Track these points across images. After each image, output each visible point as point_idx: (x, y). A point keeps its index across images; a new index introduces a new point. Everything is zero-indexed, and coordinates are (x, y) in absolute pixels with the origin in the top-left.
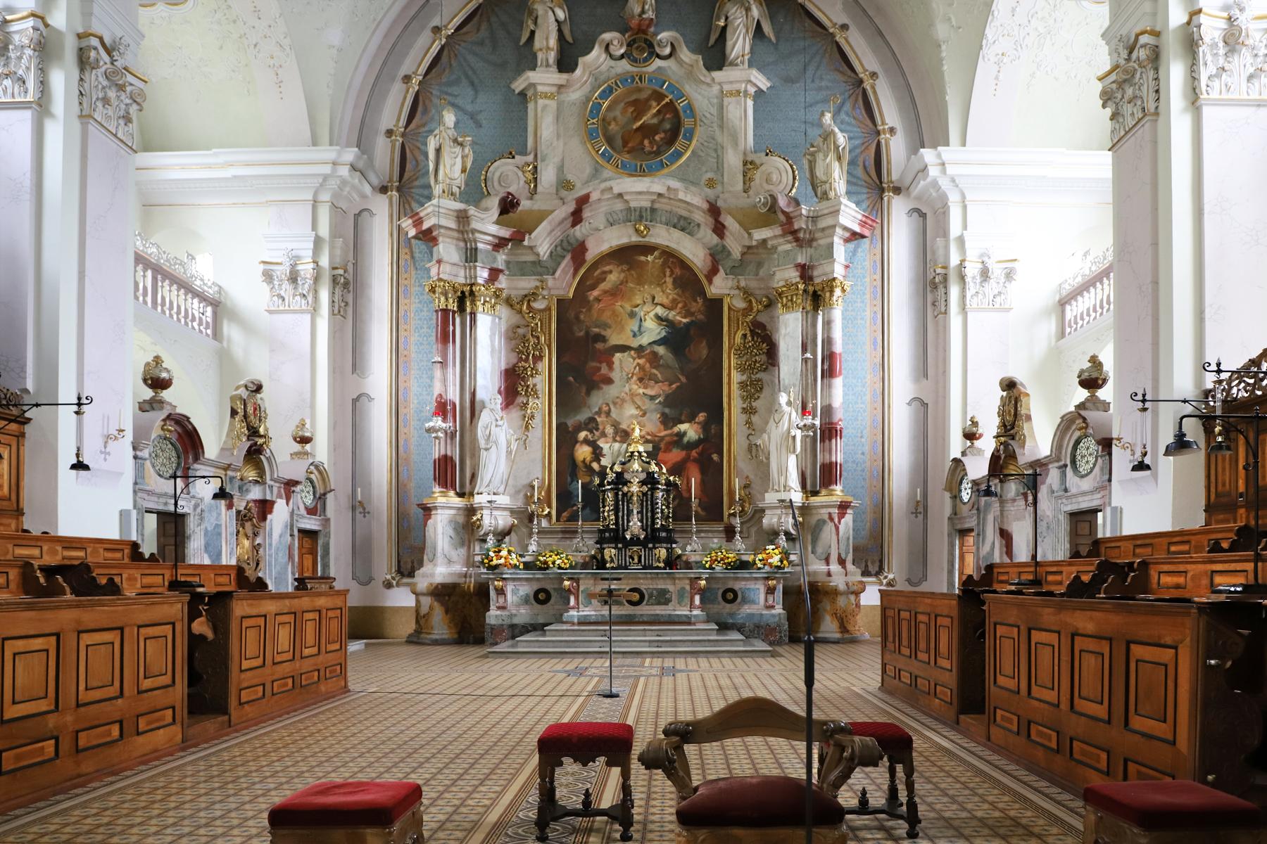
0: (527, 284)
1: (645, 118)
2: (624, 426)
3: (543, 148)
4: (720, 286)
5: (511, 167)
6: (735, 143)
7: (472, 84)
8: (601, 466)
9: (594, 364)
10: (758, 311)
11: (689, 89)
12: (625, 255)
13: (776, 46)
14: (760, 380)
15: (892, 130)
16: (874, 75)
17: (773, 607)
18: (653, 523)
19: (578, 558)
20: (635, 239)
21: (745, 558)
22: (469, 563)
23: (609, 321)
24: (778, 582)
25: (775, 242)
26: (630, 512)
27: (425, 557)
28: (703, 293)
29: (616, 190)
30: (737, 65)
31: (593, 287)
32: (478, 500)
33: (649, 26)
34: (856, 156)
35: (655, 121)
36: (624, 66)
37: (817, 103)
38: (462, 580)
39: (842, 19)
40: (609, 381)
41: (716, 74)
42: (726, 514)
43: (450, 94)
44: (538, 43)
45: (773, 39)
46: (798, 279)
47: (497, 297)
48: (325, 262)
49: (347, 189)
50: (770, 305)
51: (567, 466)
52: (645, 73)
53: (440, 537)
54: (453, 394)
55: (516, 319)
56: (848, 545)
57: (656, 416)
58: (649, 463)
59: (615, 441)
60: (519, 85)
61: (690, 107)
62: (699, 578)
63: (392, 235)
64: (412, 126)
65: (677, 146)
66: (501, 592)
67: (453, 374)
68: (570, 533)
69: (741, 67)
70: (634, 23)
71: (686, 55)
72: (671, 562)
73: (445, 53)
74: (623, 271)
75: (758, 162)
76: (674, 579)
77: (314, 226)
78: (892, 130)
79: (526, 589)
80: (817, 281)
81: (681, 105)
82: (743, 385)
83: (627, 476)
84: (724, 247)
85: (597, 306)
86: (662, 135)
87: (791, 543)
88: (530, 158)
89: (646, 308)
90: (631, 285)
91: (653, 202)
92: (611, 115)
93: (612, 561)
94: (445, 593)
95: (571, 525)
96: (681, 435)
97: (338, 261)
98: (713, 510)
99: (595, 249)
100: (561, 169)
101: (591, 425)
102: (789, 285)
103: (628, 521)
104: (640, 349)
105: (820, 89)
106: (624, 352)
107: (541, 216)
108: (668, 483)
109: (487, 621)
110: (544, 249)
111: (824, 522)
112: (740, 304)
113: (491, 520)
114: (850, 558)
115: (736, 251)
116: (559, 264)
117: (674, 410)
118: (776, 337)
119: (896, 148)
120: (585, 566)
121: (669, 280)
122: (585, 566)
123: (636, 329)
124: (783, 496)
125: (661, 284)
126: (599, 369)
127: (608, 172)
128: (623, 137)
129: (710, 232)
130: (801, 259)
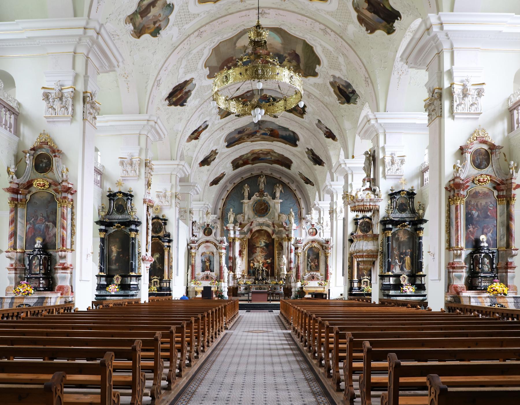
0: (243, 236)
3: (245, 212)
4: (274, 236)
11: (269, 202)
12: (258, 231)
15: (303, 208)
16: (300, 199)
20: (260, 228)
22: (234, 283)
28: (271, 237)
36: (259, 198)
39: (295, 189)
40: (256, 253)
44: (245, 194)
51: (249, 267)
54: (232, 256)
55: (241, 242)
60: (242, 201)
61: (269, 206)
65: (267, 212)
66: (240, 288)
67: (232, 252)
68: (249, 278)
70: (261, 191)
71: (269, 197)
78: (303, 208)
79: (244, 288)
82: (278, 253)
95: (250, 277)
96: (268, 262)
98: (273, 275)
99: (254, 230)
100: (248, 216)
101: (253, 260)
104: (261, 247)
107: (245, 225)
112: (277, 239)
113: (238, 276)
117: (267, 257)
119: (304, 211)
125: (264, 236)
127: (256, 217)
130: (287, 233)
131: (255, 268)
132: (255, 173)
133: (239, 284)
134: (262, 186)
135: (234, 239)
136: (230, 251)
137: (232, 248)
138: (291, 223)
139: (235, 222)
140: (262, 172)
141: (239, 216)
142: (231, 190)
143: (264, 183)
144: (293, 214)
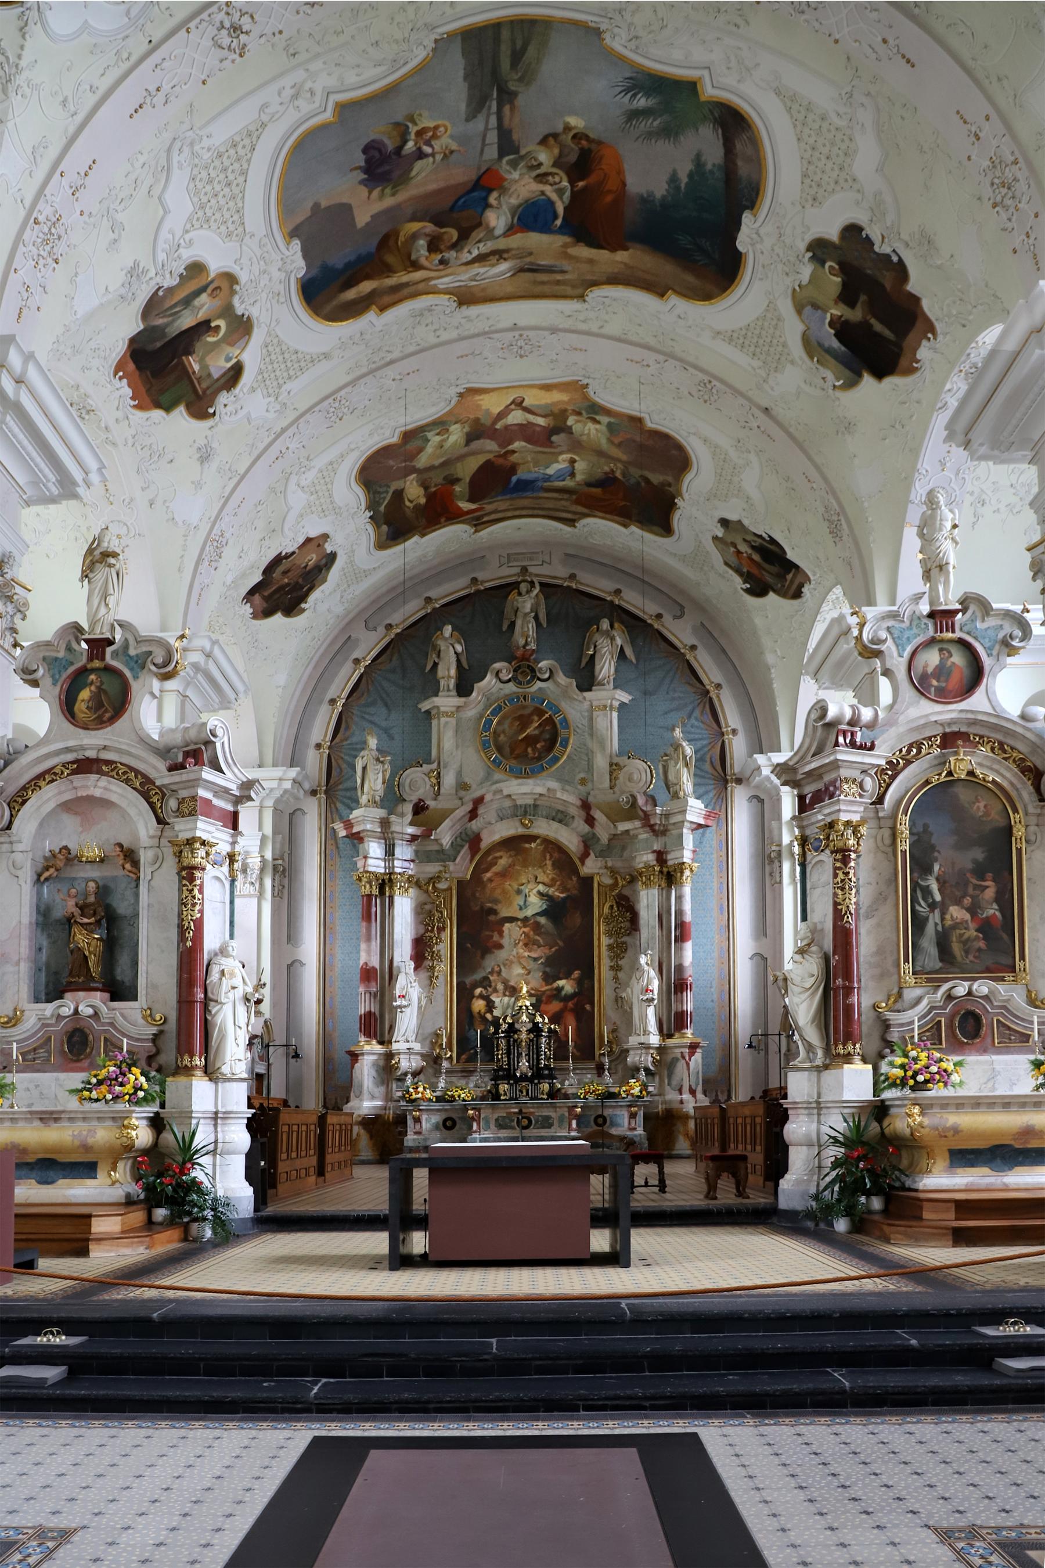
0: (433, 868)
1: (528, 731)
2: (512, 983)
3: (444, 757)
4: (591, 866)
5: (420, 774)
6: (602, 747)
7: (386, 705)
8: (494, 1017)
9: (487, 933)
10: (623, 886)
11: (564, 705)
12: (512, 844)
13: (636, 666)
14: (625, 943)
17: (635, 1129)
18: (538, 1063)
19: (479, 1092)
20: (521, 831)
21: (612, 1090)
22: (388, 1097)
23: (500, 897)
24: (640, 1109)
25: (635, 832)
26: (519, 1055)
27: (352, 1094)
28: (576, 872)
29: (505, 793)
30: (604, 685)
31: (487, 870)
32: (395, 1046)
33: (531, 655)
34: (705, 754)
35: (537, 732)
36: (511, 687)
37: (672, 711)
38: (382, 1112)
39: (691, 640)
40: (500, 947)
41: (587, 694)
42: (597, 1053)
43: (368, 714)
44: (441, 672)
45: (634, 660)
46: (655, 863)
47: (410, 882)
48: (269, 855)
49: (287, 796)
50: (633, 880)
51: (466, 1017)
52: (529, 693)
53: (366, 1077)
54: (375, 962)
55: (423, 897)
56: (698, 1078)
57: (539, 974)
58: (534, 1015)
59: (505, 995)
60: (425, 706)
61: (565, 721)
62: (576, 1107)
63: (320, 830)
64: (337, 740)
65: (555, 752)
67: (376, 945)
68: (467, 1073)
69: (607, 687)
70: (519, 653)
71: (562, 679)
72: (553, 1094)
73: (364, 679)
74: (511, 856)
75: (622, 765)
76: (555, 1107)
77: (260, 829)
78: (734, 732)
79: (436, 1118)
80: (670, 863)
81: (557, 719)
82: (610, 947)
83: (517, 1026)
84: (594, 834)
85: (490, 886)
86: (543, 744)
87: (650, 1078)
88: (434, 766)
89: (530, 886)
90: (517, 867)
91: (535, 800)
92: (500, 728)
93: (505, 1094)
94: (371, 1123)
95: (470, 1066)
96: (560, 989)
97: (278, 852)
98: (586, 1051)
99: (488, 839)
100: (459, 774)
101: (485, 983)
102: (648, 866)
103: (518, 1062)
104: (526, 919)
105: (673, 699)
106: (511, 922)
107: (444, 815)
108: (550, 1030)
109: (405, 1144)
110: (446, 841)
111: (677, 1059)
112: (608, 881)
113: (405, 1064)
114: (700, 1089)
115: (604, 838)
116: (459, 852)
117: (553, 969)
118: (637, 907)
120: (483, 1098)
121: (549, 863)
122: (483, 1098)
123: (522, 903)
124: (642, 1039)
126: (492, 937)
127: (497, 776)
128: (510, 747)
129: (582, 822)
131: (496, 1023)
132: (492, 575)
133: (412, 1101)
134: (526, 633)
135: (385, 884)
136: (368, 939)
137: (375, 928)
138: (675, 796)
139: (392, 799)
140: (524, 570)
141: (414, 774)
142: (374, 660)
143: (536, 618)
144: (689, 750)
